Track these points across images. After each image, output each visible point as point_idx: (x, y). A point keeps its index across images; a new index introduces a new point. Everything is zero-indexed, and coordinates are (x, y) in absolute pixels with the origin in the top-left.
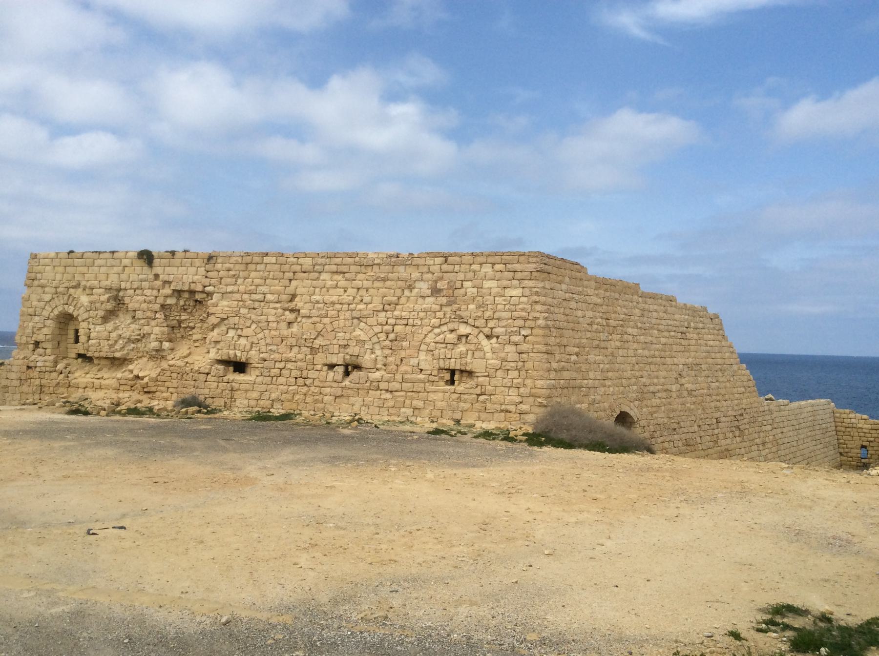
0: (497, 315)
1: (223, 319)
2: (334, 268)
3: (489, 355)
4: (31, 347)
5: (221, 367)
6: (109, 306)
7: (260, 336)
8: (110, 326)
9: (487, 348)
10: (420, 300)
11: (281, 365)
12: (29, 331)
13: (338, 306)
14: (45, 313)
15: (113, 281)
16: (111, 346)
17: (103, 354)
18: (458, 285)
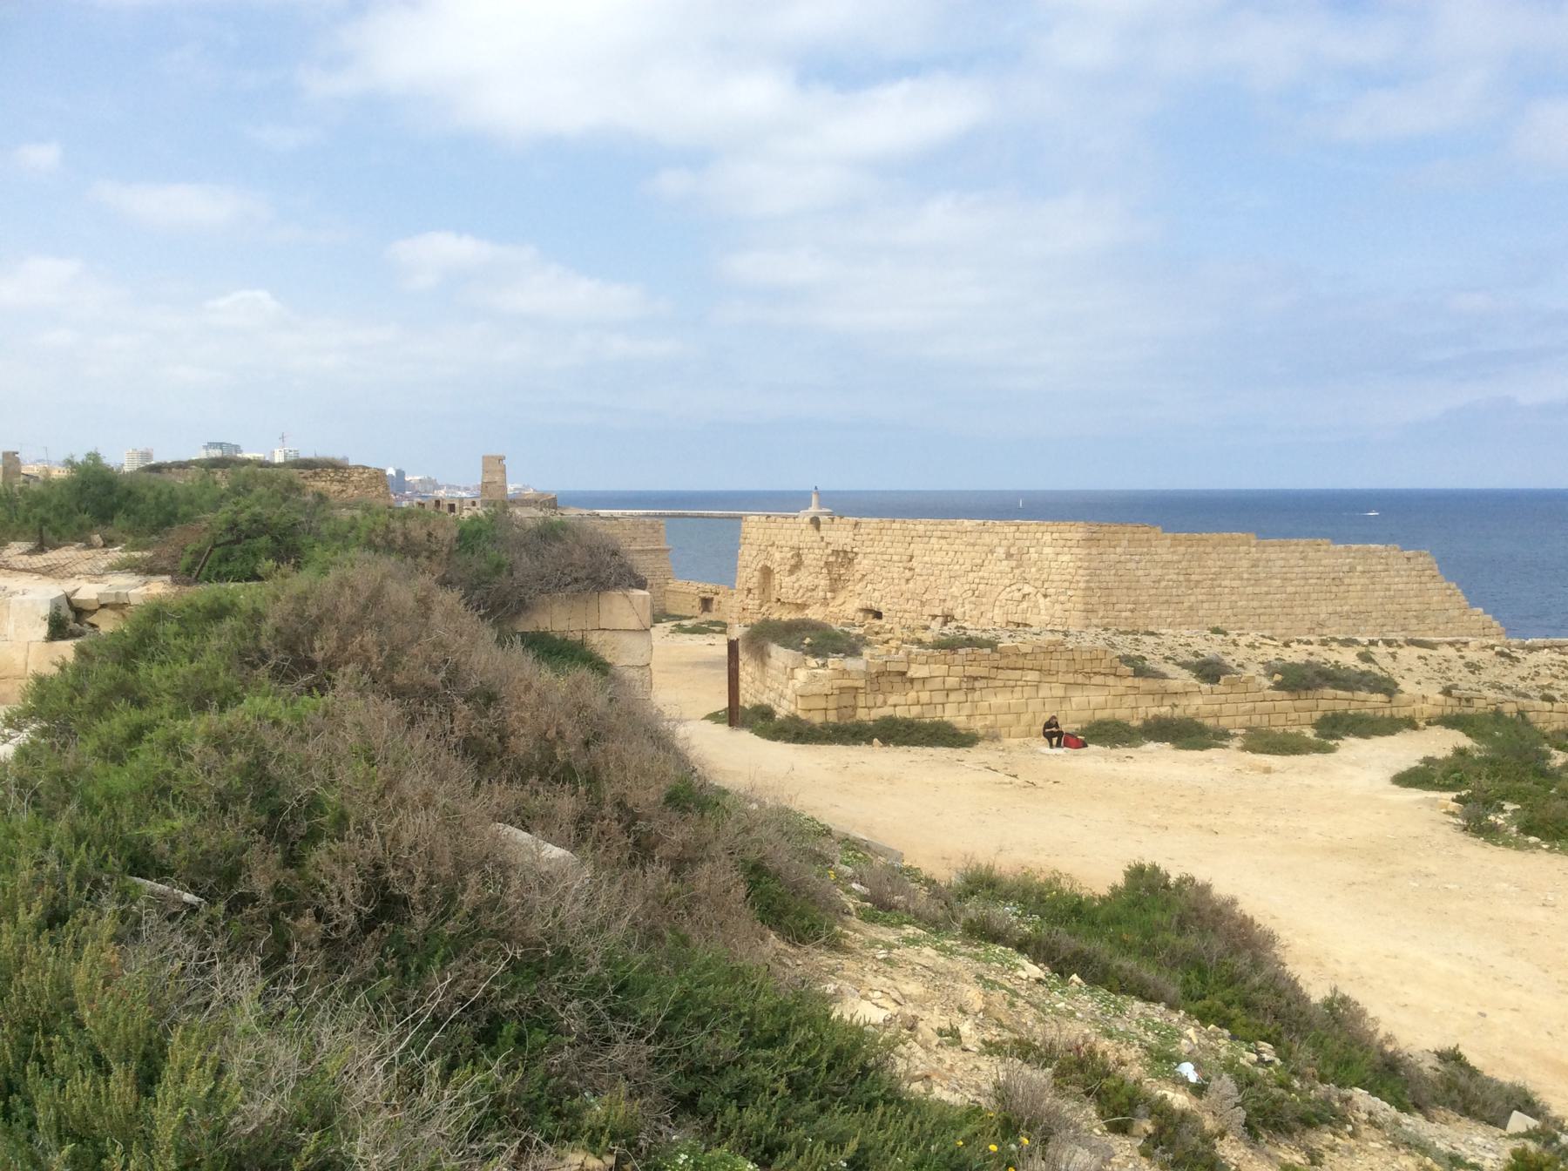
0: (1050, 578)
1: (864, 576)
2: (939, 534)
3: (1043, 612)
4: (746, 592)
5: (861, 614)
6: (793, 562)
7: (888, 590)
8: (794, 578)
9: (1042, 606)
10: (998, 563)
11: (899, 615)
12: (744, 580)
13: (940, 567)
14: (753, 566)
15: (794, 542)
16: (795, 594)
17: (790, 600)
18: (1025, 550)
